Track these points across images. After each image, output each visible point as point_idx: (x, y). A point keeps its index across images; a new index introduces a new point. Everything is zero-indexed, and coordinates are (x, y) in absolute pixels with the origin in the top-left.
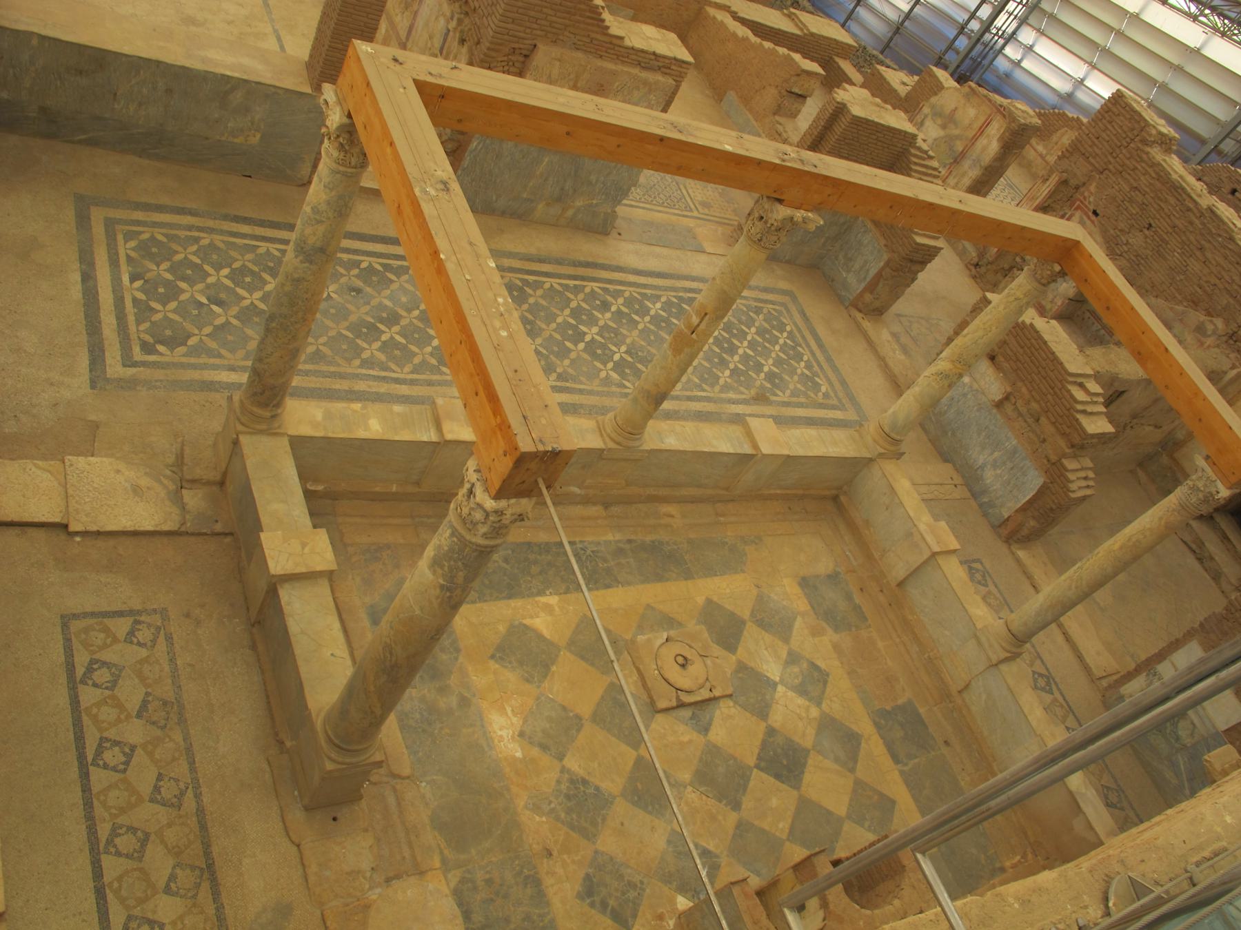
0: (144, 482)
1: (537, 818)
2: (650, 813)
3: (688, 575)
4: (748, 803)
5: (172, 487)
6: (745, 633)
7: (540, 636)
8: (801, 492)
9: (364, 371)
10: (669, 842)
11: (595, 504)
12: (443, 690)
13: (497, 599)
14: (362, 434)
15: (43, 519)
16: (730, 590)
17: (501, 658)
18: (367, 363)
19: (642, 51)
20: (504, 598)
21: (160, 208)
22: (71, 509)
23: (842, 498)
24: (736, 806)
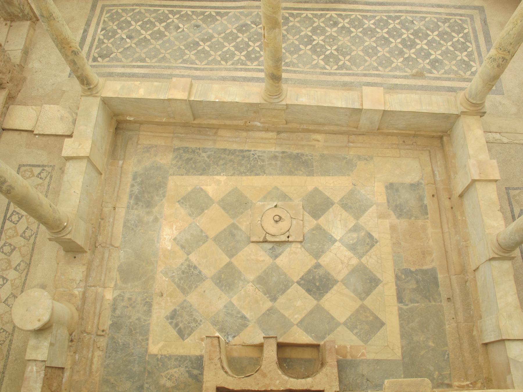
1: (164, 278)
2: (222, 290)
3: (311, 173)
4: (282, 300)
6: (331, 210)
7: (207, 195)
8: (413, 132)
10: (225, 306)
11: (272, 131)
12: (148, 213)
13: (195, 174)
14: (134, 96)
15: (26, 129)
16: (333, 185)
17: (182, 203)
18: (185, 62)
20: (198, 175)
23: (445, 139)
24: (274, 299)
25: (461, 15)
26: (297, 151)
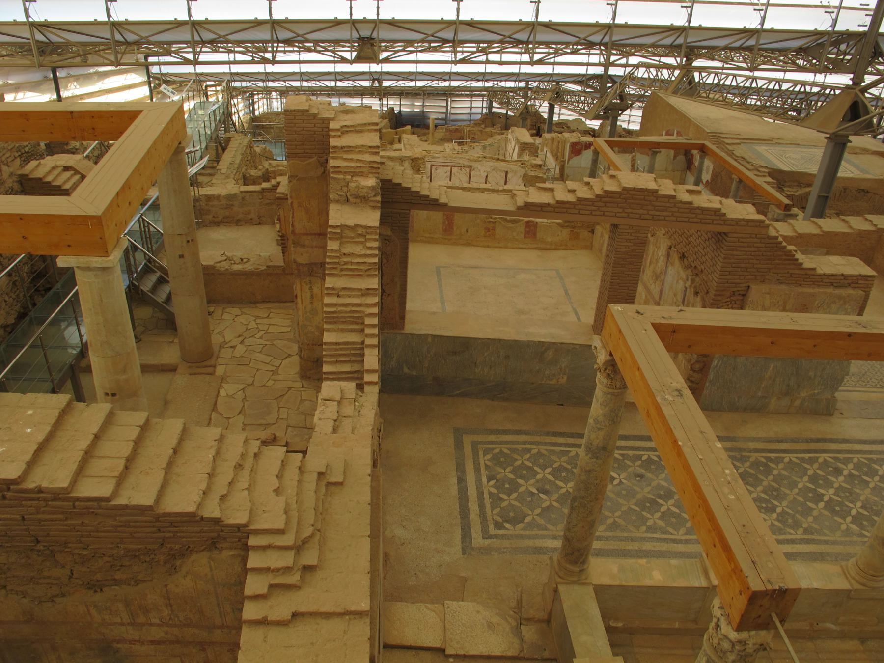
0: (496, 619)
5: (514, 624)
9: (649, 535)
14: (648, 582)
15: (430, 645)
18: (650, 529)
19: (833, 275)
21: (505, 432)
22: (447, 639)
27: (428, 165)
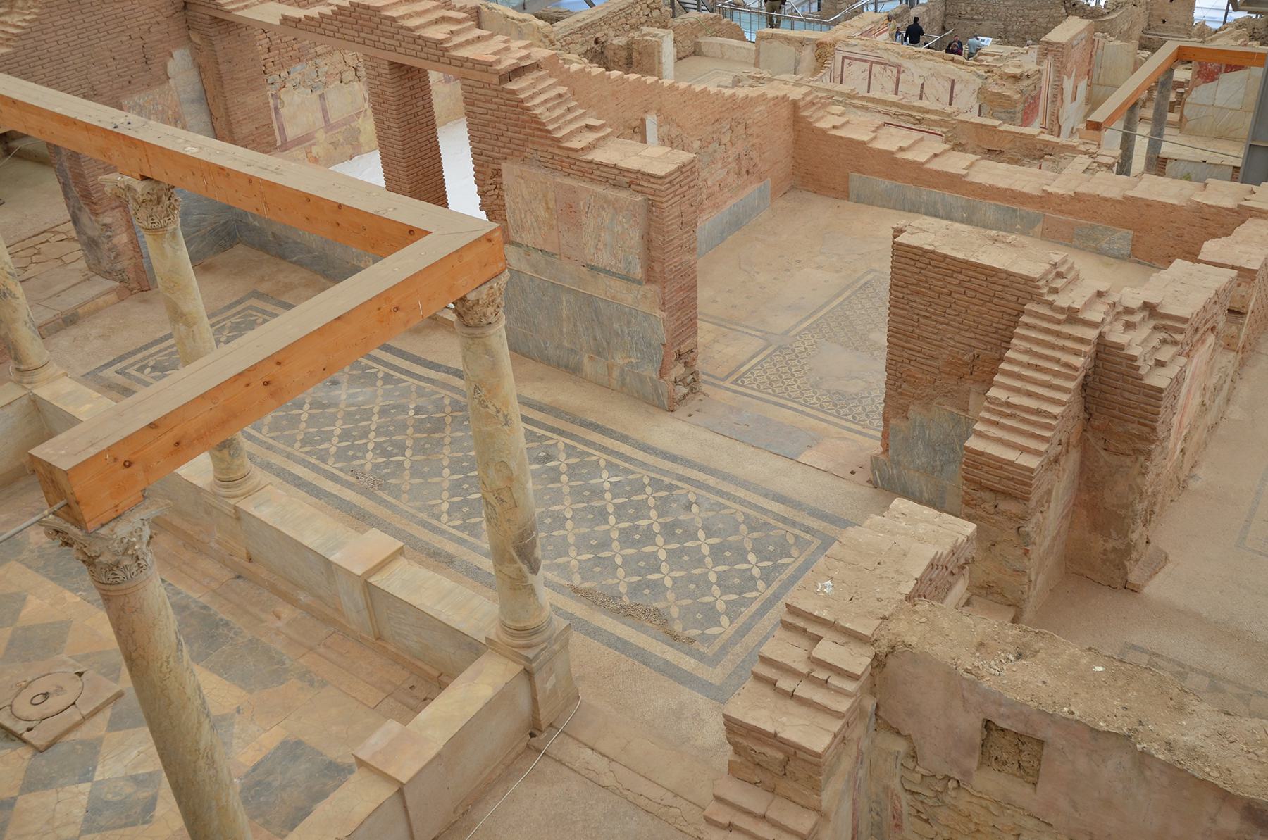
19: (601, 164)
25: (807, 530)
26: (227, 617)
27: (839, 56)
